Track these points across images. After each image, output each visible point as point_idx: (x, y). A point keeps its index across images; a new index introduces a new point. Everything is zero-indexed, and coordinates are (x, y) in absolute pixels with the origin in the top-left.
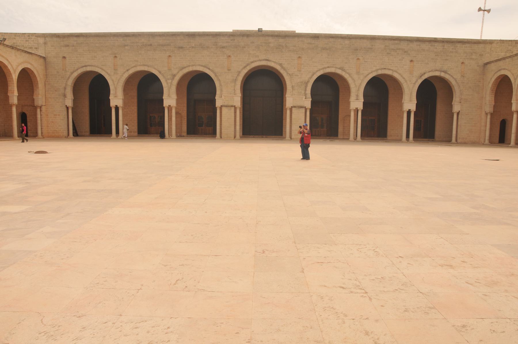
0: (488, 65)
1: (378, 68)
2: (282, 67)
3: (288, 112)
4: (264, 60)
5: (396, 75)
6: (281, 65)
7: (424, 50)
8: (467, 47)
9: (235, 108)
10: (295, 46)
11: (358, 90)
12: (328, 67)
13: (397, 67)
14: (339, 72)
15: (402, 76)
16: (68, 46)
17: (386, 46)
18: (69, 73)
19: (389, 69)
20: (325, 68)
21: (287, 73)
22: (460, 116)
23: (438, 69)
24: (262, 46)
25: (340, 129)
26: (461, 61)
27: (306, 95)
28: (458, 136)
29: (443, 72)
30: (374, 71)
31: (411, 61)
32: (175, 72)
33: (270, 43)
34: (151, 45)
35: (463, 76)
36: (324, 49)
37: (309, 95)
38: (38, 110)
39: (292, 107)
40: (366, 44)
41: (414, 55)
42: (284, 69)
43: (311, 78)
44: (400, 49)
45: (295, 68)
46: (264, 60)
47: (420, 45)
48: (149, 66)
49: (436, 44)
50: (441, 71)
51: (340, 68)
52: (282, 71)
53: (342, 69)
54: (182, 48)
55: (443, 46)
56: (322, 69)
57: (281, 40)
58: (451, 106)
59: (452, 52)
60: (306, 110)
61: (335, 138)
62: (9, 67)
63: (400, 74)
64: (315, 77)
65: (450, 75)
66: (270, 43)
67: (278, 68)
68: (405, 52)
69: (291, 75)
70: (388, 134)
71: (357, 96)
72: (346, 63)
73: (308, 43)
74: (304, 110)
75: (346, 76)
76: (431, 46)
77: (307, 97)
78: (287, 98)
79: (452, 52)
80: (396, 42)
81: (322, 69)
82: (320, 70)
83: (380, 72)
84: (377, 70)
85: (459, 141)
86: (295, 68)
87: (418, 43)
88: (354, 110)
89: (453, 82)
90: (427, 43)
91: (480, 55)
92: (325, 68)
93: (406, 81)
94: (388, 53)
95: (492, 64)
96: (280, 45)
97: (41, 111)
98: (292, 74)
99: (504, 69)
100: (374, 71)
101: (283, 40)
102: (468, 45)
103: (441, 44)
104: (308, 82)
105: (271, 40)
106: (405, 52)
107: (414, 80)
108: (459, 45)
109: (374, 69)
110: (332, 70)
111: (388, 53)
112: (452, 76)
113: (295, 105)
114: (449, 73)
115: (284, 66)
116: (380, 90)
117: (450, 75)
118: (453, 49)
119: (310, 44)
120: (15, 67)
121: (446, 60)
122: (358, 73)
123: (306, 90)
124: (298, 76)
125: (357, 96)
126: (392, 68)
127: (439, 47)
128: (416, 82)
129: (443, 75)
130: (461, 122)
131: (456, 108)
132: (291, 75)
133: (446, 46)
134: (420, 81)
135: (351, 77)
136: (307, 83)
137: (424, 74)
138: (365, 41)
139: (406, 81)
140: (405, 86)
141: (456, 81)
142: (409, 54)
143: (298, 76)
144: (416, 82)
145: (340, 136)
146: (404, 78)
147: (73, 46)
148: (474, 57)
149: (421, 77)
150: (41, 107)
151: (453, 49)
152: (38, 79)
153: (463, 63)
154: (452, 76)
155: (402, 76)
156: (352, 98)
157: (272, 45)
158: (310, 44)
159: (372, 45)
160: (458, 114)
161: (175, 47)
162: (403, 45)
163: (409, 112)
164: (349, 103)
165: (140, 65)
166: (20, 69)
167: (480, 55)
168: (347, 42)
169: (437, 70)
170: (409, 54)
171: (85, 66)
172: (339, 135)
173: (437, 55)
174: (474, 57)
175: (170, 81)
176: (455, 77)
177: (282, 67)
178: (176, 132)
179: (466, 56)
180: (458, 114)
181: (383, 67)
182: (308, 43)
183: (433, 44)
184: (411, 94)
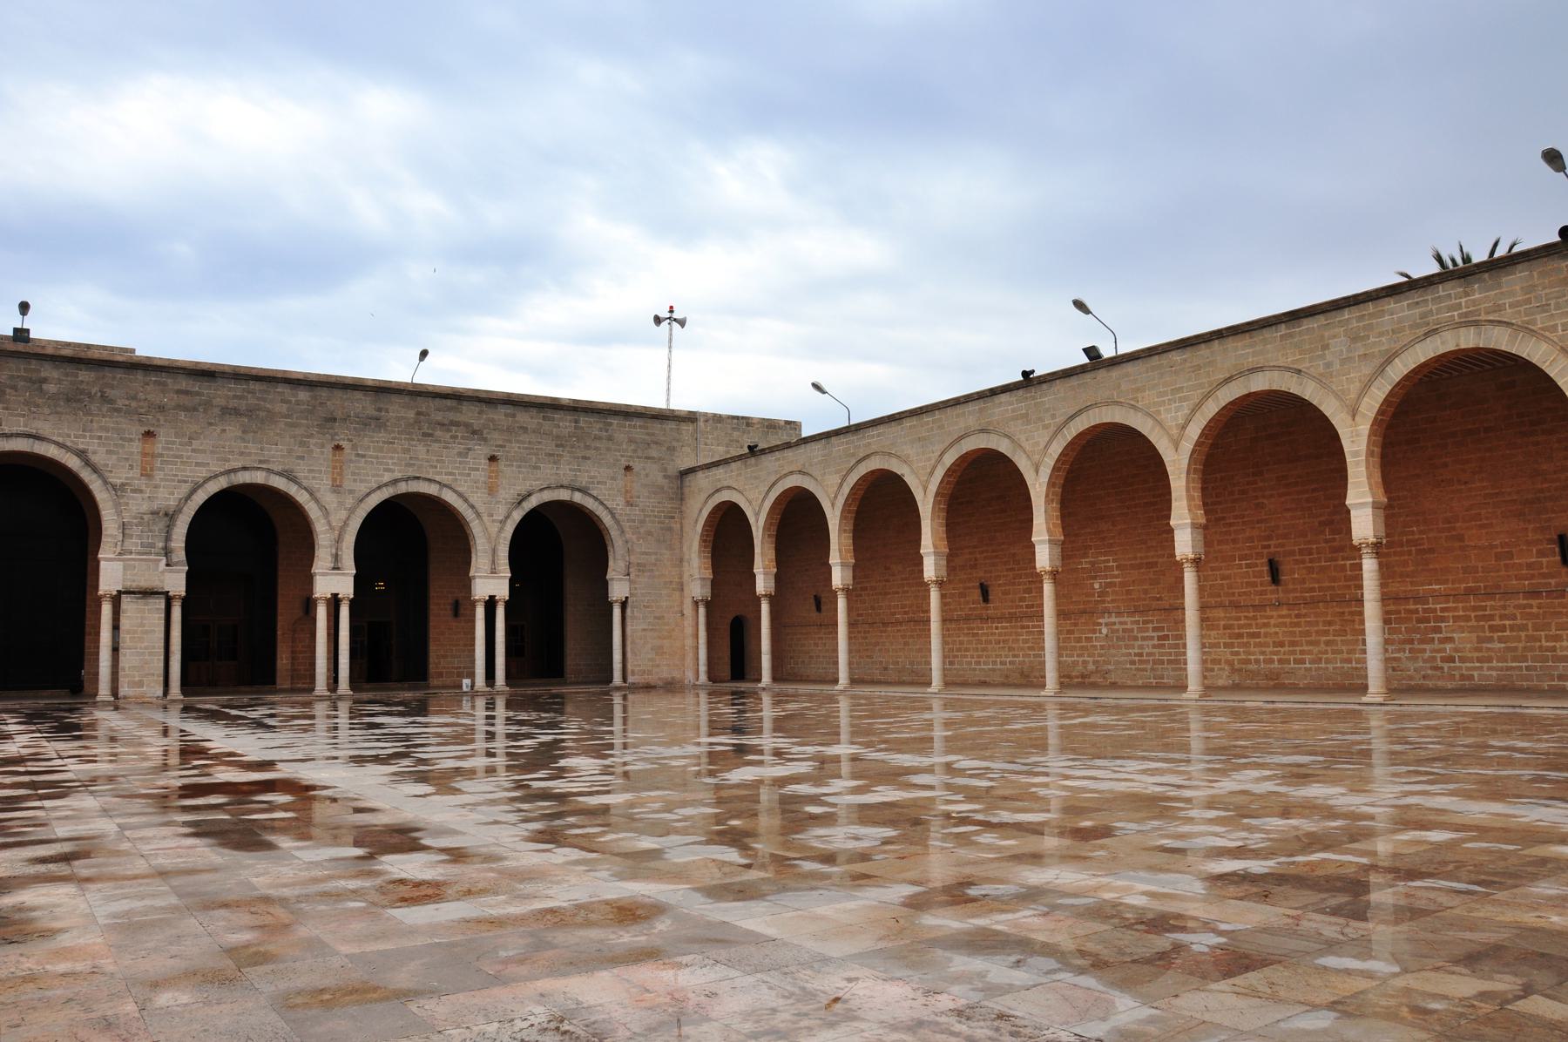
0: (690, 477)
1: (398, 475)
2: (88, 463)
3: (106, 610)
4: (18, 435)
5: (449, 497)
6: (81, 454)
7: (525, 429)
9: (169, 601)
10: (134, 398)
11: (339, 540)
12: (245, 469)
13: (451, 474)
14: (279, 483)
15: (466, 500)
17: (419, 413)
19: (430, 480)
20: (234, 471)
21: (105, 482)
22: (629, 611)
23: (565, 483)
24: (14, 388)
25: (283, 661)
26: (624, 462)
27: (167, 552)
28: (629, 667)
29: (579, 490)
30: (386, 485)
31: (493, 459)
33: (45, 380)
35: (629, 504)
36: (226, 411)
37: (180, 554)
39: (119, 592)
40: (362, 405)
42: (95, 470)
43: (188, 498)
44: (457, 424)
45: (131, 467)
46: (18, 435)
47: (514, 416)
50: (574, 489)
51: (279, 474)
52: (86, 475)
53: (289, 476)
56: (222, 474)
57: (85, 375)
58: (605, 585)
60: (169, 601)
61: (267, 688)
63: (460, 495)
64: (201, 498)
65: (596, 499)
66: (45, 380)
67: (73, 462)
68: (474, 432)
69: (117, 490)
70: (432, 668)
71: (336, 557)
72: (302, 458)
73: (178, 392)
74: (161, 603)
75: (302, 497)
77: (175, 559)
78: (102, 564)
80: (449, 402)
81: (222, 474)
82: (216, 476)
83: (403, 488)
84: (395, 482)
85: (631, 679)
86: (131, 467)
87: (510, 410)
88: (328, 601)
90: (534, 411)
92: (234, 471)
93: (478, 515)
94: (424, 435)
95: (700, 474)
96: (82, 392)
98: (123, 485)
99: (729, 488)
100: (386, 485)
101: (93, 375)
102: (638, 422)
104: (178, 511)
105: (48, 371)
106: (474, 432)
108: (615, 421)
109: (387, 478)
110: (258, 478)
111: (424, 435)
112: (602, 503)
113: (133, 585)
114: (594, 493)
115: (94, 458)
116: (408, 539)
117: (596, 499)
119: (187, 393)
121: (585, 458)
122: (336, 488)
123: (168, 539)
124: (141, 491)
125: (336, 557)
126: (437, 478)
127: (565, 424)
128: (507, 517)
129: (578, 498)
131: (618, 590)
132: (117, 490)
133: (584, 420)
134: (517, 516)
135: (317, 501)
136: (171, 517)
138: (358, 395)
139: (478, 515)
140: (476, 528)
142: (485, 440)
143: (141, 491)
144: (507, 517)
145: (283, 681)
146: (472, 507)
148: (654, 453)
153: (628, 468)
154: (602, 503)
155: (466, 500)
156: (322, 562)
157: (51, 388)
158: (187, 393)
159: (380, 410)
160: (624, 605)
162: (469, 414)
163: (491, 604)
164: (309, 580)
168: (303, 395)
170: (485, 440)
172: (278, 681)
174: (654, 453)
177: (88, 463)
179: (635, 451)
180: (624, 605)
181: (411, 472)
182: (178, 392)
184: (494, 551)
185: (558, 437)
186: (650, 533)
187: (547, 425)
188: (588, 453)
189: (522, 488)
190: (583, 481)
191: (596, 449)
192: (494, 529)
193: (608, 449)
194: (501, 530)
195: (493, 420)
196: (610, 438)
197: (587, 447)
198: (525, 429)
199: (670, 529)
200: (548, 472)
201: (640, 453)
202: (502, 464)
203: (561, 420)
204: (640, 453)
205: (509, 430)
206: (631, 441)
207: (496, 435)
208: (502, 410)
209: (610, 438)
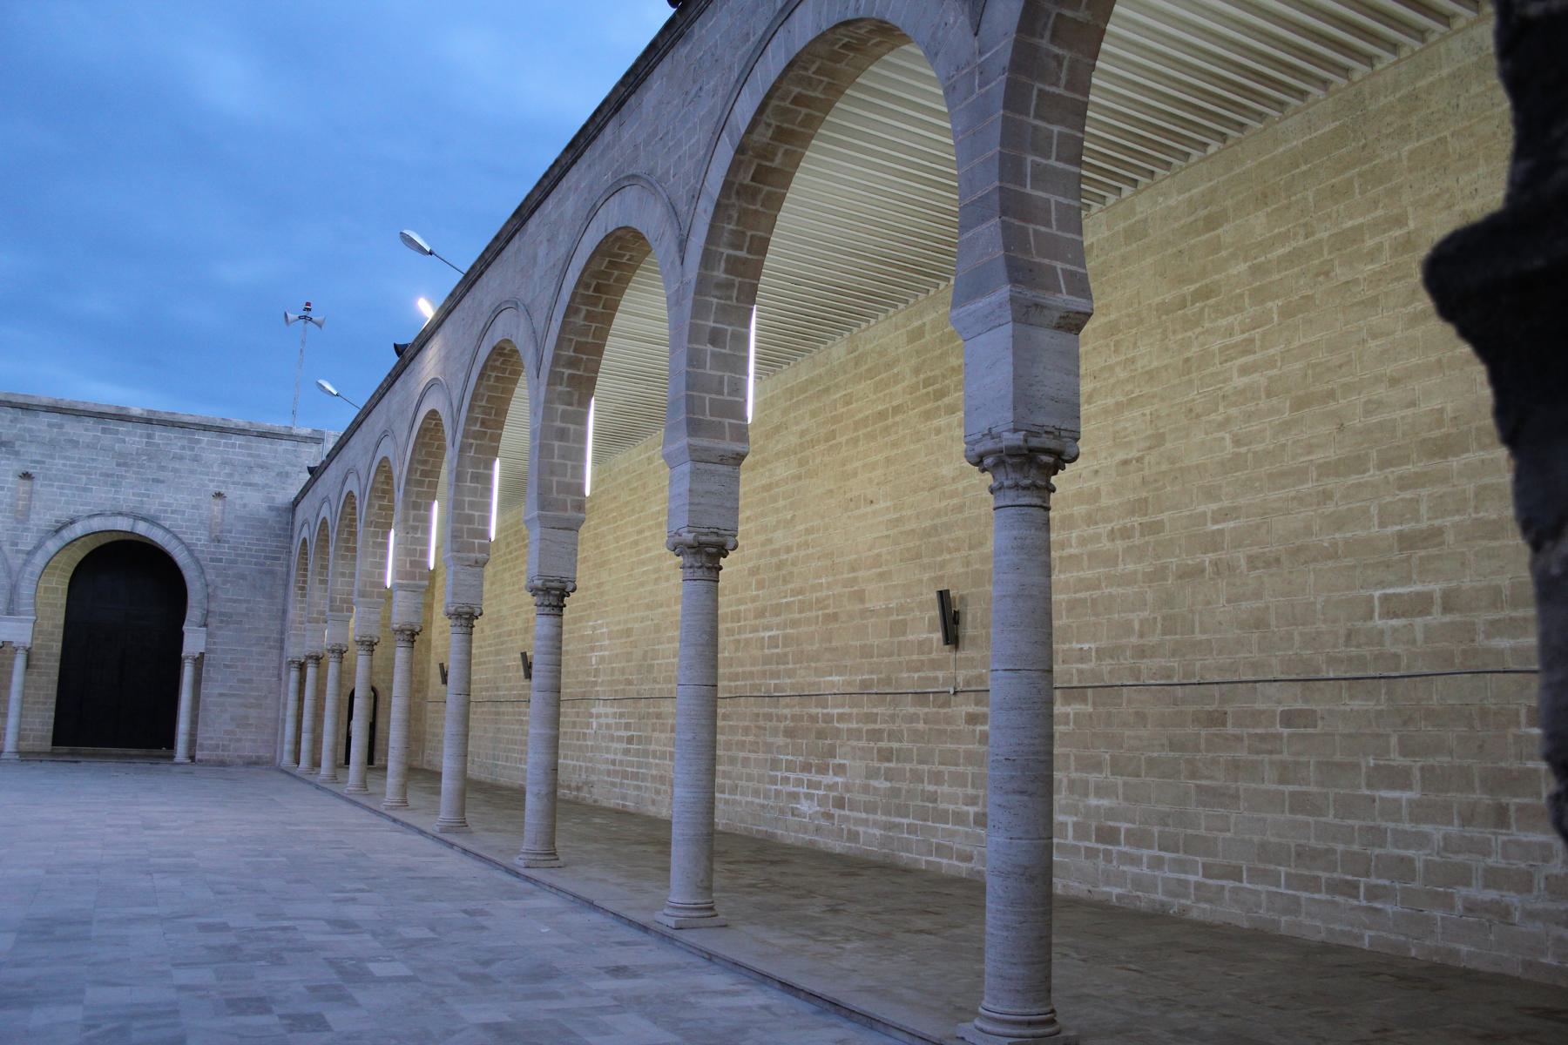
7: (75, 444)
8: (233, 445)
23: (124, 510)
26: (213, 488)
41: (38, 458)
47: (61, 427)
49: (124, 428)
50: (137, 518)
55: (149, 436)
59: (181, 458)
65: (167, 530)
76: (104, 431)
79: (181, 458)
87: (56, 418)
89: (181, 557)
90: (90, 422)
91: (279, 474)
102: (238, 440)
103: (140, 430)
107: (28, 541)
108: (205, 438)
114: (167, 524)
117: (167, 530)
118: (183, 448)
127: (133, 439)
128: (37, 548)
129: (142, 528)
130: (210, 690)
133: (159, 435)
134: (52, 546)
137: (72, 522)
141: (191, 552)
142: (17, 453)
144: (37, 548)
148: (257, 478)
149: (57, 531)
151: (183, 448)
167: (279, 474)
169: (120, 514)
170: (17, 453)
173: (125, 464)
174: (257, 478)
176: (186, 538)
179: (230, 475)
183: (112, 425)
185: (121, 454)
186: (243, 577)
187: (107, 440)
188: (161, 475)
189: (63, 514)
190: (152, 507)
191: (175, 471)
192: (17, 561)
193: (192, 472)
194: (26, 563)
195: (30, 430)
196: (196, 459)
197: (162, 468)
198: (75, 444)
199: (271, 573)
200: (101, 496)
201: (236, 478)
202: (38, 485)
203: (128, 433)
204: (236, 478)
205: (53, 444)
206: (225, 463)
207: (33, 448)
208: (45, 418)
209: (196, 459)
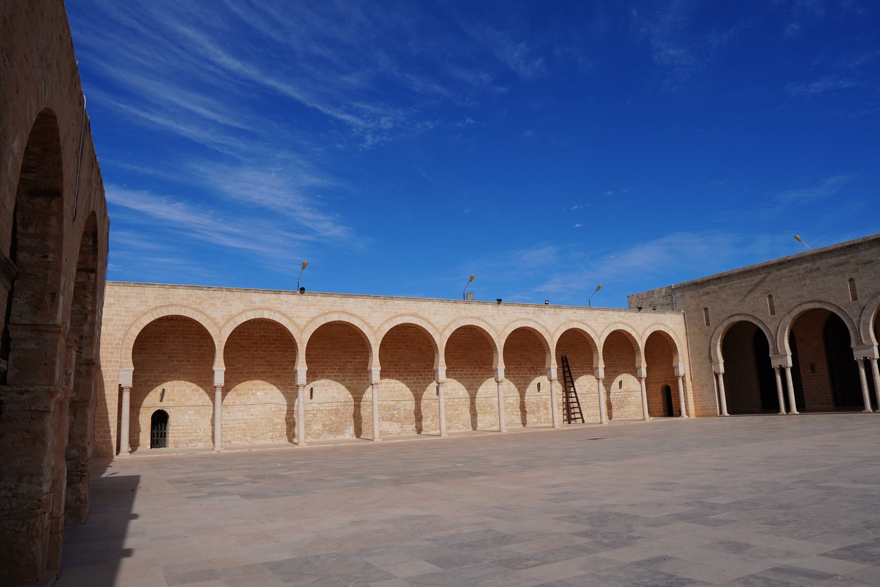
16: (708, 293)
18: (713, 328)
32: (862, 302)
34: (818, 269)
38: (680, 381)
48: (820, 302)
54: (870, 262)
62: (634, 334)
97: (684, 382)
120: (640, 332)
147: (715, 292)
150: (683, 377)
152: (676, 342)
161: (857, 264)
165: (806, 303)
166: (648, 333)
171: (732, 316)
175: (857, 319)
178: (696, 410)
